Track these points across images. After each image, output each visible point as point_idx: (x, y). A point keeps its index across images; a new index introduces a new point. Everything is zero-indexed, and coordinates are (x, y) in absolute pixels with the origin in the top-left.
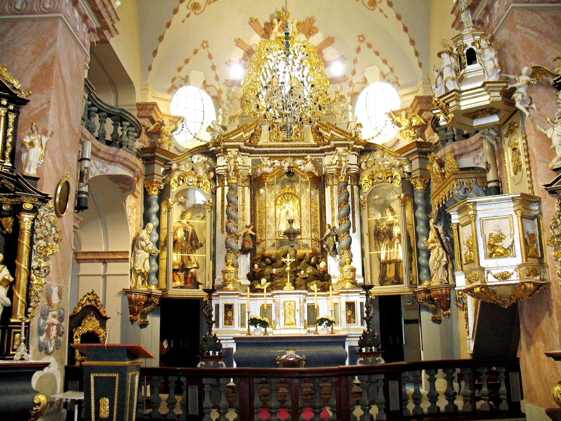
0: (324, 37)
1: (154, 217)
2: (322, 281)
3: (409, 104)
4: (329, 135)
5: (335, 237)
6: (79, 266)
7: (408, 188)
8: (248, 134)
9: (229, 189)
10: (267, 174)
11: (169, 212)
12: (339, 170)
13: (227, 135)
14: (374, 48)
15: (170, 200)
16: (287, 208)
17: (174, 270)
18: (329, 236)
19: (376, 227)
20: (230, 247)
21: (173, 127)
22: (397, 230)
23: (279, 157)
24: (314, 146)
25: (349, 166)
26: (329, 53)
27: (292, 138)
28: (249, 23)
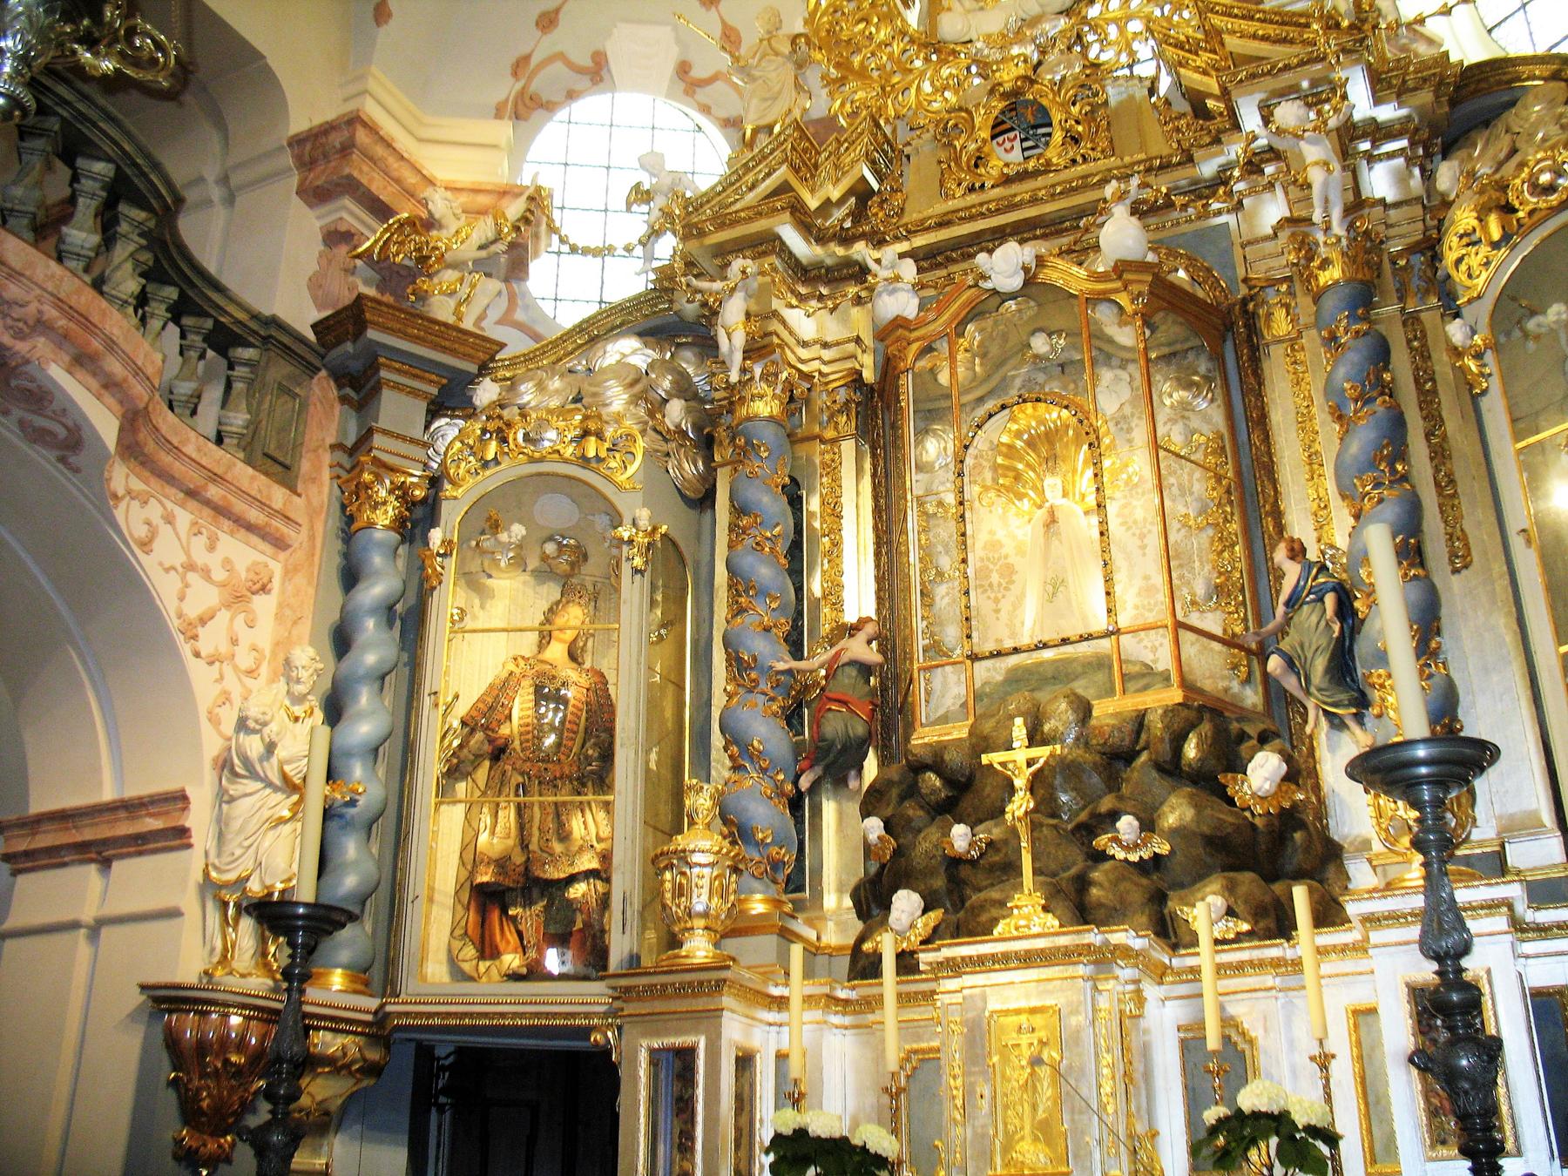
5: (1330, 600)
6: (13, 885)
18: (1293, 602)
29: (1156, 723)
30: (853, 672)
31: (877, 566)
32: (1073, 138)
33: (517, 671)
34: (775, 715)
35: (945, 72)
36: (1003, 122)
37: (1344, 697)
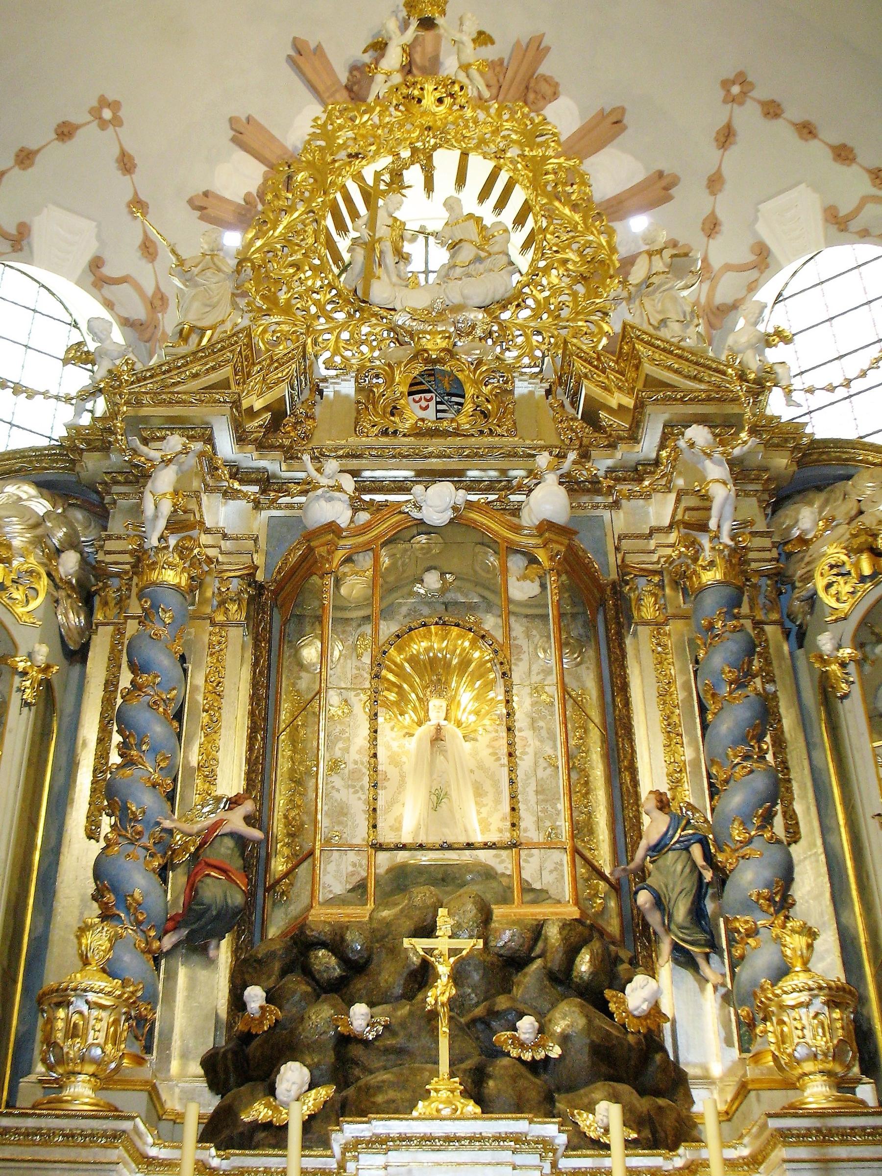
2: (642, 1092)
5: (696, 851)
14: (793, 113)
18: (658, 849)
29: (553, 932)
30: (229, 843)
31: (250, 748)
32: (482, 412)
34: (154, 870)
35: (365, 329)
36: (421, 383)
37: (701, 937)
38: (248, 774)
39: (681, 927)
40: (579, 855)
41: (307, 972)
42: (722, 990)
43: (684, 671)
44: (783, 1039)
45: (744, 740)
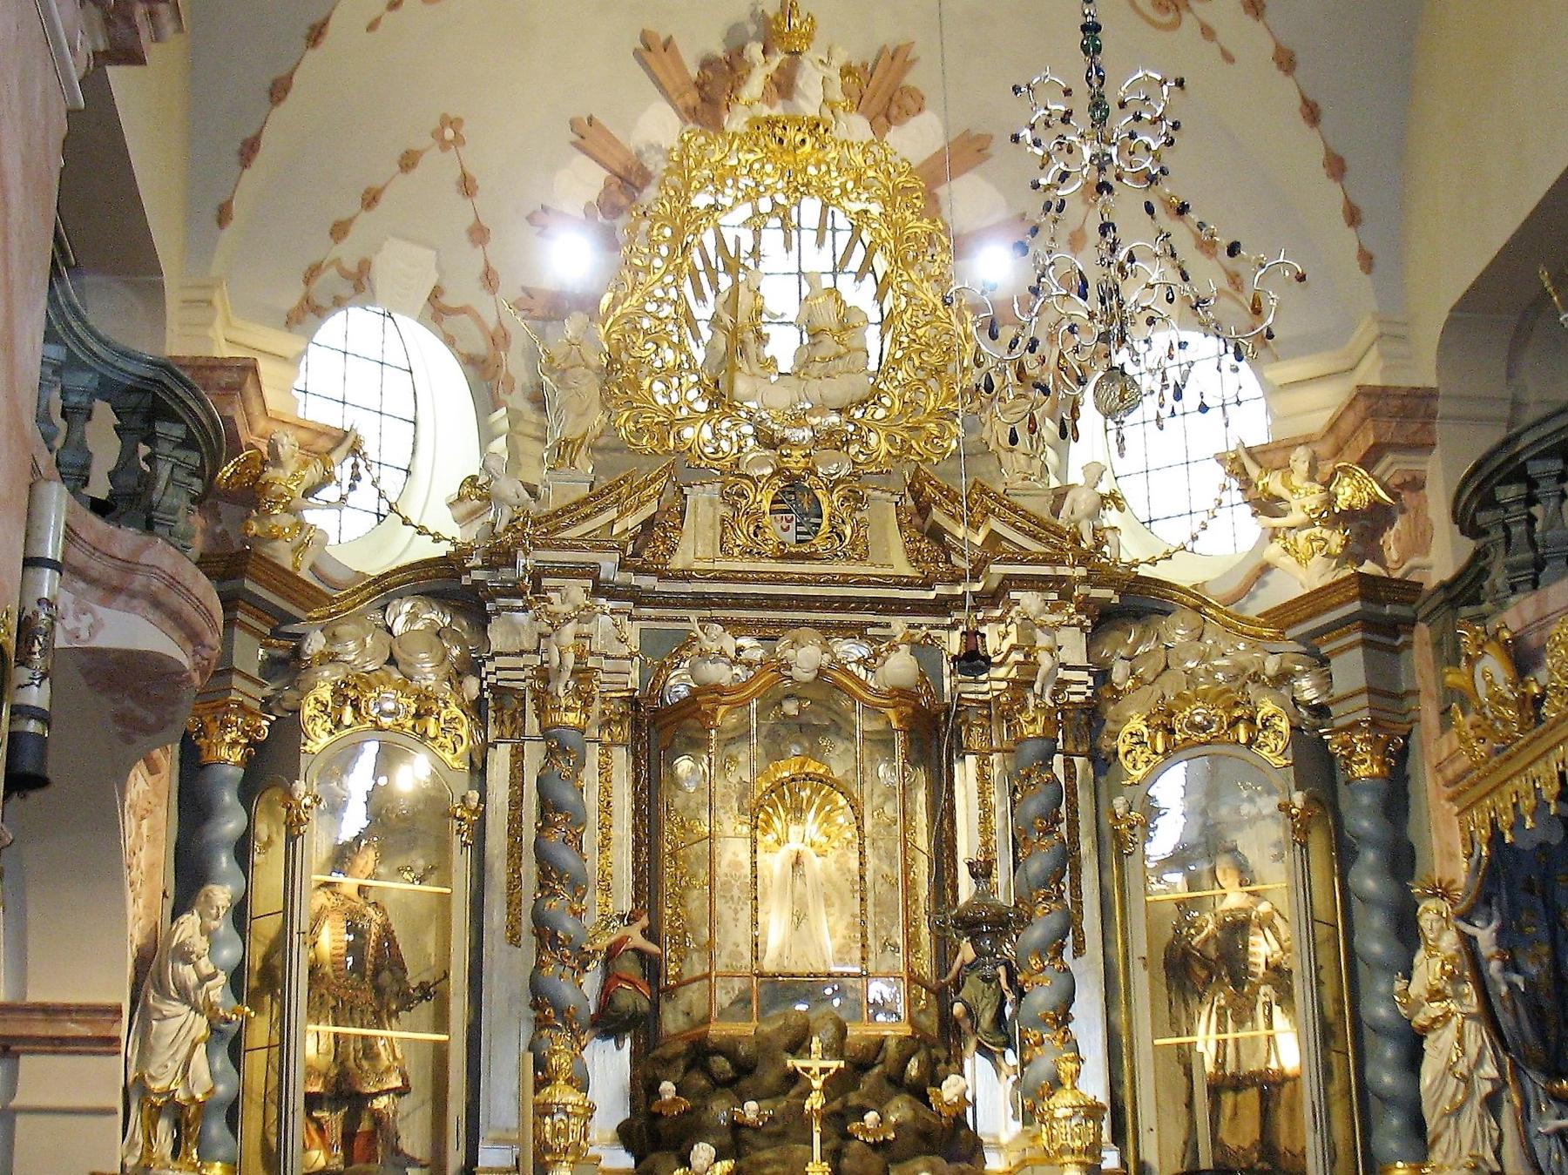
0: (947, 135)
1: (225, 861)
3: (1317, 422)
4: (978, 540)
5: (1001, 970)
7: (1316, 764)
8: (632, 521)
9: (550, 753)
10: (718, 689)
11: (291, 839)
12: (1021, 686)
13: (548, 517)
15: (300, 786)
16: (794, 845)
17: (312, 1101)
18: (972, 966)
19: (1177, 929)
20: (553, 1005)
21: (312, 474)
22: (1262, 949)
23: (759, 623)
24: (910, 584)
25: (1062, 674)
26: (971, 199)
27: (819, 544)
28: (636, 53)
29: (891, 1044)
33: (329, 905)
37: (1001, 1039)
38: (636, 884)
39: (985, 1032)
40: (914, 979)
41: (707, 1071)
42: (1013, 1078)
43: (1002, 801)
44: (1051, 1139)
45: (1046, 885)
